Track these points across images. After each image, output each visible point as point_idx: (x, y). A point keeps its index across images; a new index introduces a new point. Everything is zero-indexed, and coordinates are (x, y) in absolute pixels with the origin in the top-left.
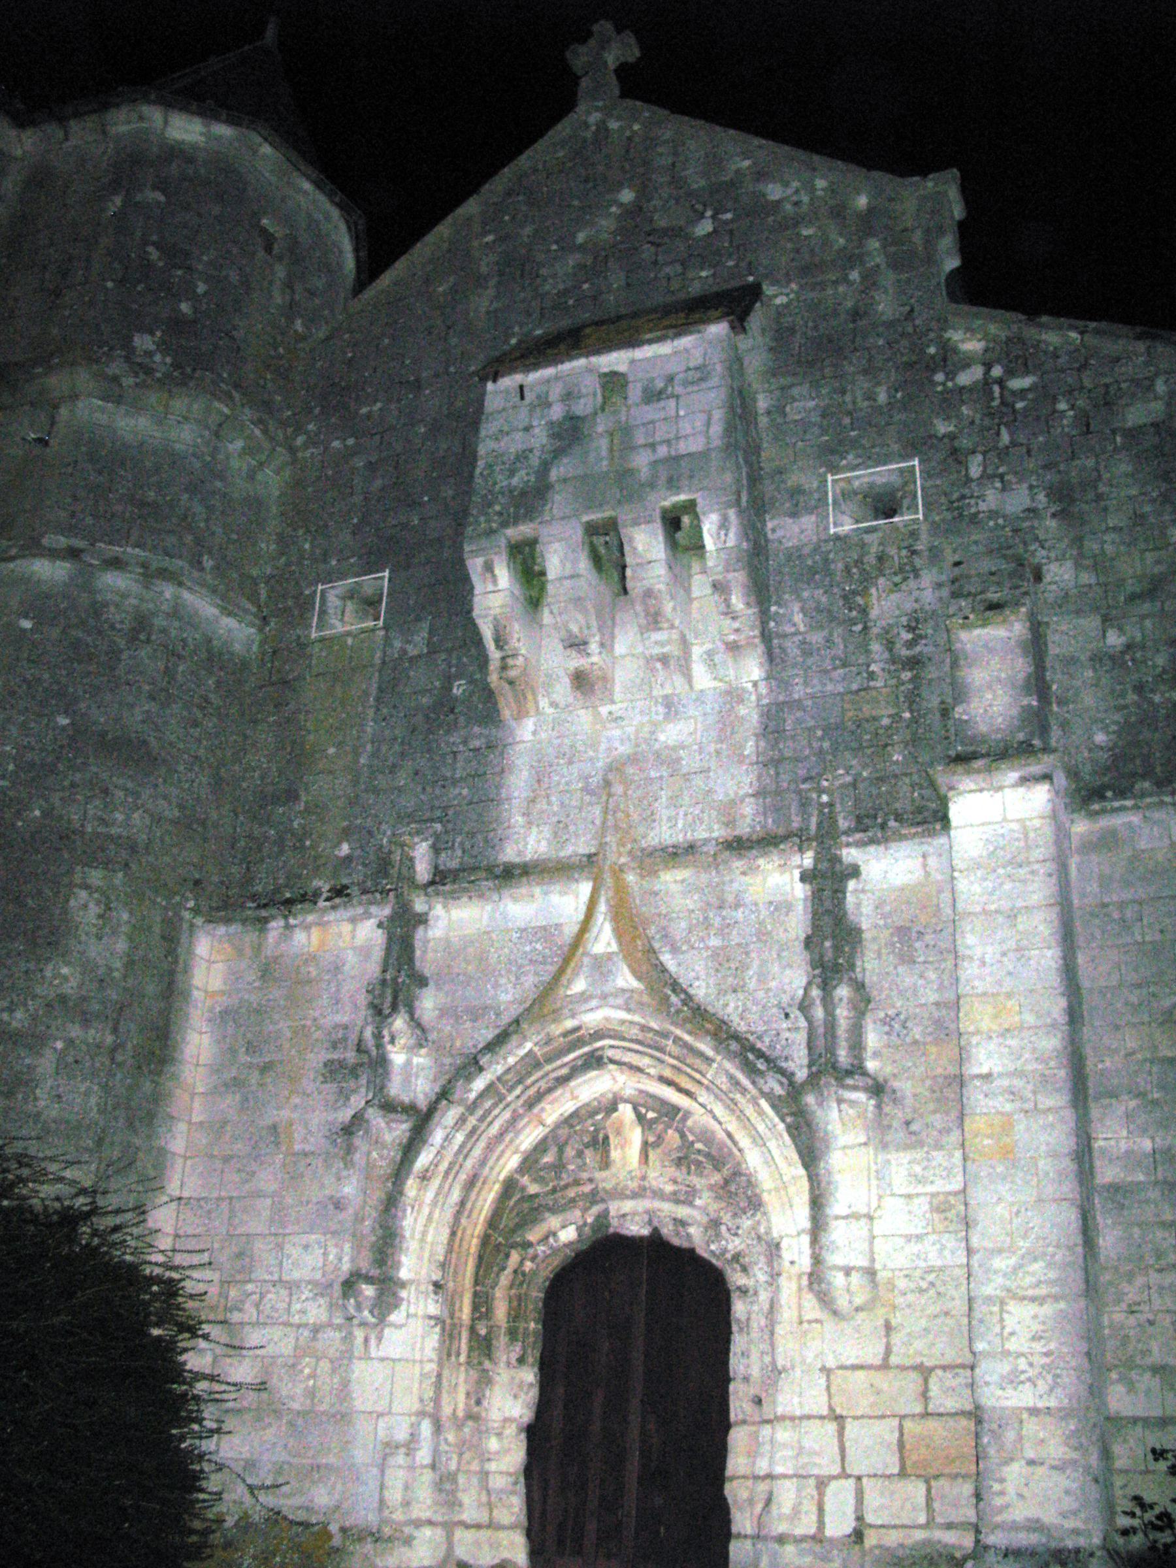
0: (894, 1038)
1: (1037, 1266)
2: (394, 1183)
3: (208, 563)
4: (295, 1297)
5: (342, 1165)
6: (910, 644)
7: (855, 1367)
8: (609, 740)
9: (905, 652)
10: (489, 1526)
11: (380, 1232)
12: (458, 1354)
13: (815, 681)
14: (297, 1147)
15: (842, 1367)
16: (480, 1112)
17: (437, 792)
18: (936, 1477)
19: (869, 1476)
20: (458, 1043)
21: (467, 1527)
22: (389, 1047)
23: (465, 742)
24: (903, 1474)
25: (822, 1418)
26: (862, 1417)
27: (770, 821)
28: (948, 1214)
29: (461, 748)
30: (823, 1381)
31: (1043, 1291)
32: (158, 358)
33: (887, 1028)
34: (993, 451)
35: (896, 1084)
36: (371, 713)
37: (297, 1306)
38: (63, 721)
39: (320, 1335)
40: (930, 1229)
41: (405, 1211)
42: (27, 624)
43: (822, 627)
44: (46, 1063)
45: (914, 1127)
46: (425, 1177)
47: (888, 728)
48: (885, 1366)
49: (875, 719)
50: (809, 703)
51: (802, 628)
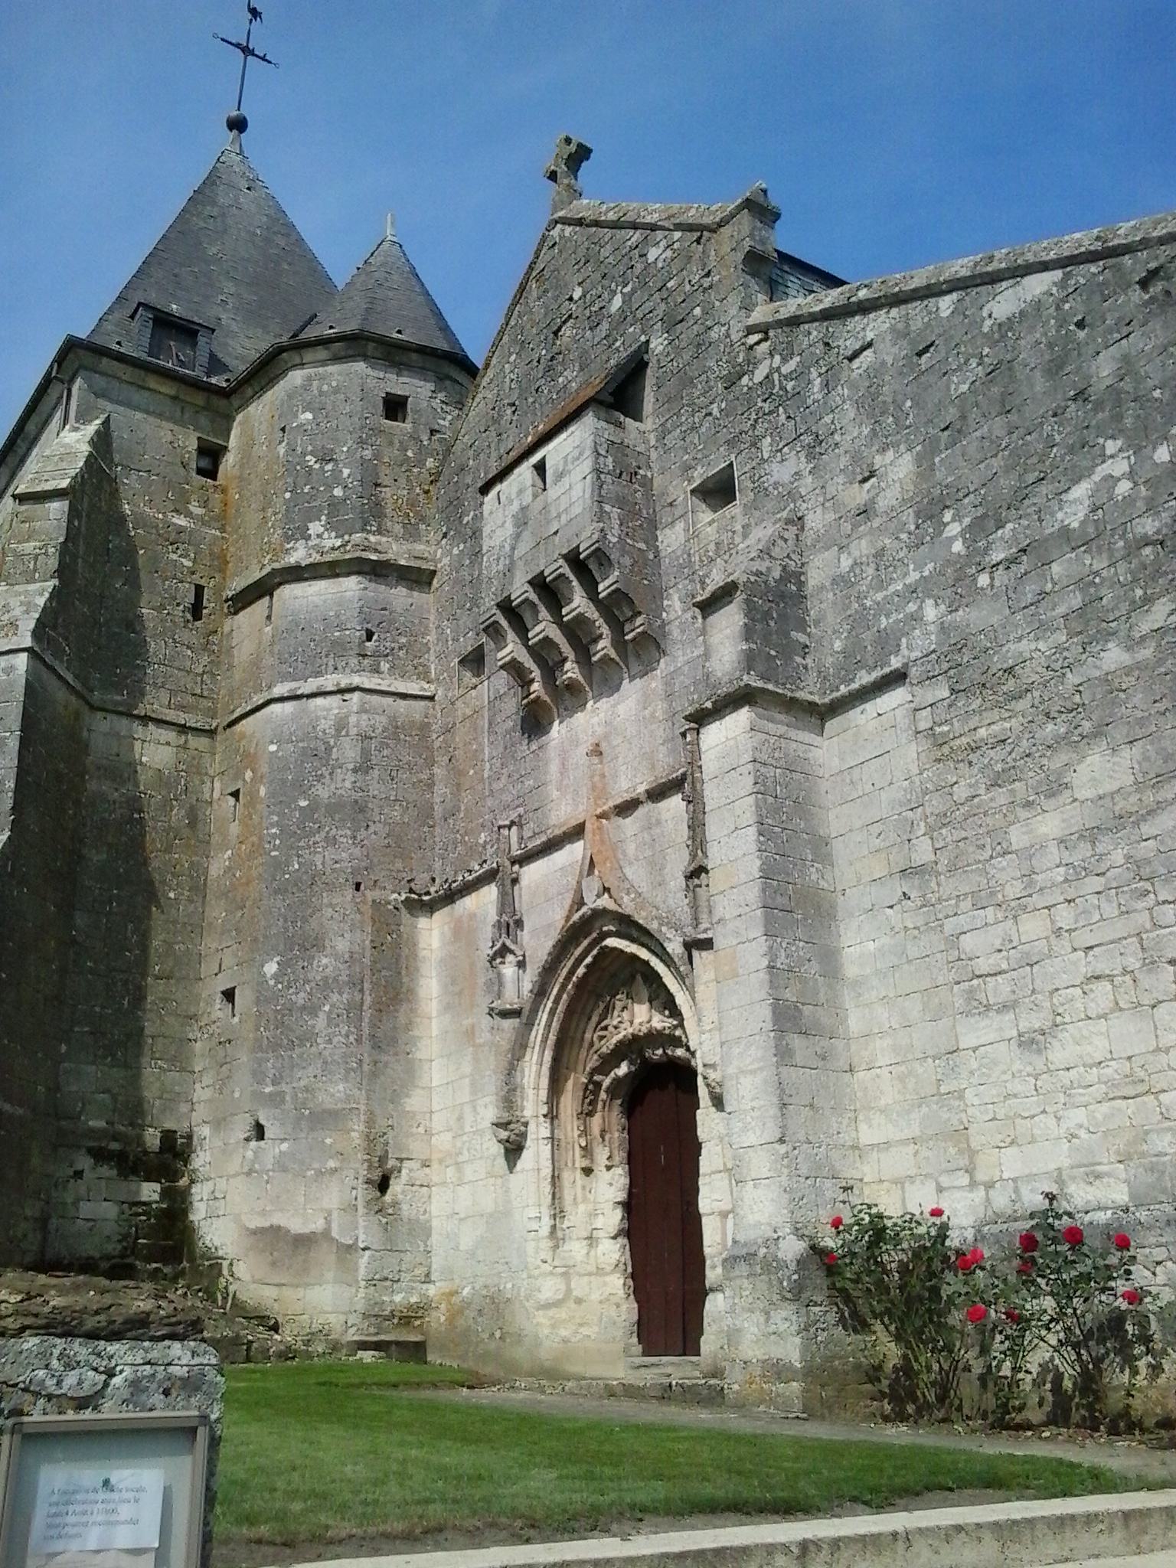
1: (752, 1051)
3: (385, 666)
10: (596, 1274)
21: (580, 1275)
31: (756, 1066)
32: (326, 535)
34: (775, 431)
38: (303, 803)
42: (273, 748)
44: (321, 1022)
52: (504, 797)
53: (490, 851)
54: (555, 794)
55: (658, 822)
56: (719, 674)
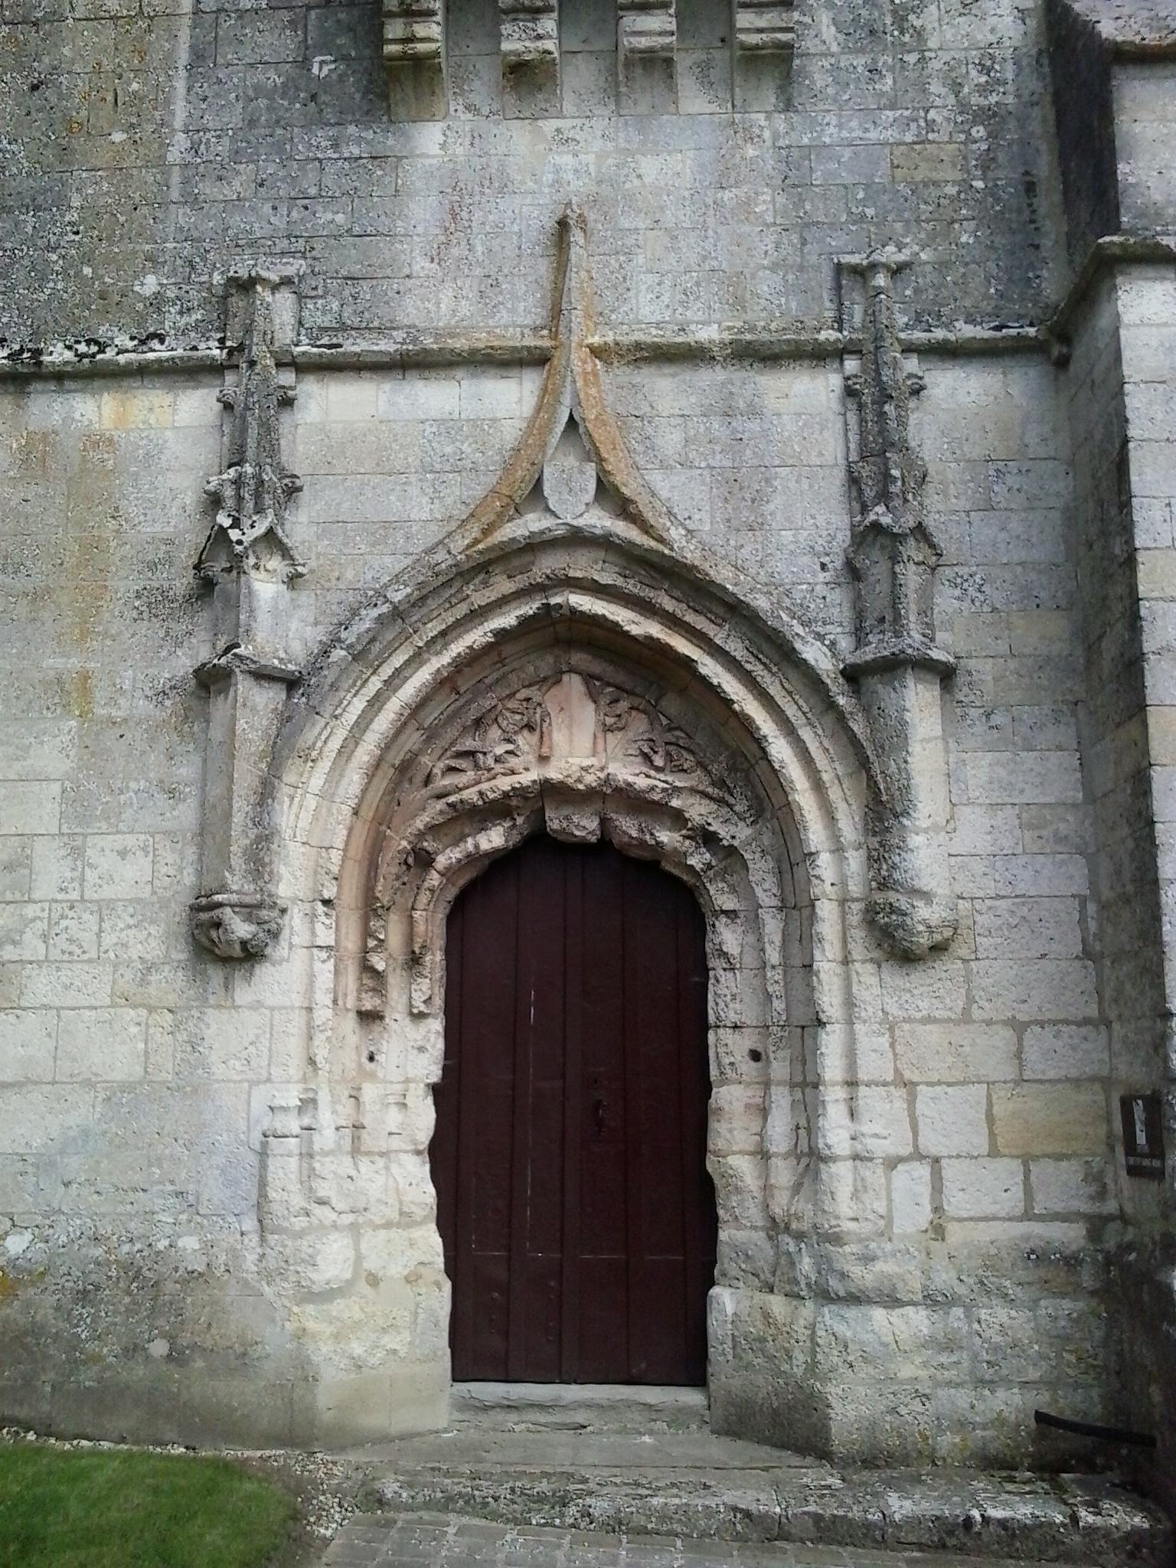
0: (967, 604)
2: (269, 766)
4: (106, 925)
5: (176, 738)
6: (983, 90)
7: (929, 1020)
8: (557, 170)
9: (976, 100)
10: (398, 1225)
11: (253, 833)
12: (346, 995)
13: (854, 124)
14: (101, 711)
15: (908, 1020)
16: (386, 671)
17: (295, 214)
18: (1036, 1158)
19: (950, 1157)
20: (349, 574)
21: (376, 1227)
22: (253, 573)
23: (335, 146)
24: (994, 1153)
25: (885, 1084)
26: (939, 1083)
27: (794, 305)
28: (1044, 833)
29: (330, 153)
30: (885, 1041)
33: (957, 592)
35: (972, 664)
36: (180, 86)
37: (108, 940)
39: (154, 978)
40: (1019, 850)
41: (281, 804)
43: (862, 51)
45: (997, 719)
46: (308, 758)
47: (952, 199)
48: (966, 1018)
49: (936, 184)
50: (847, 153)
51: (835, 48)
52: (237, 221)
53: (172, 318)
54: (421, 265)
55: (754, 412)
56: (1157, 197)
